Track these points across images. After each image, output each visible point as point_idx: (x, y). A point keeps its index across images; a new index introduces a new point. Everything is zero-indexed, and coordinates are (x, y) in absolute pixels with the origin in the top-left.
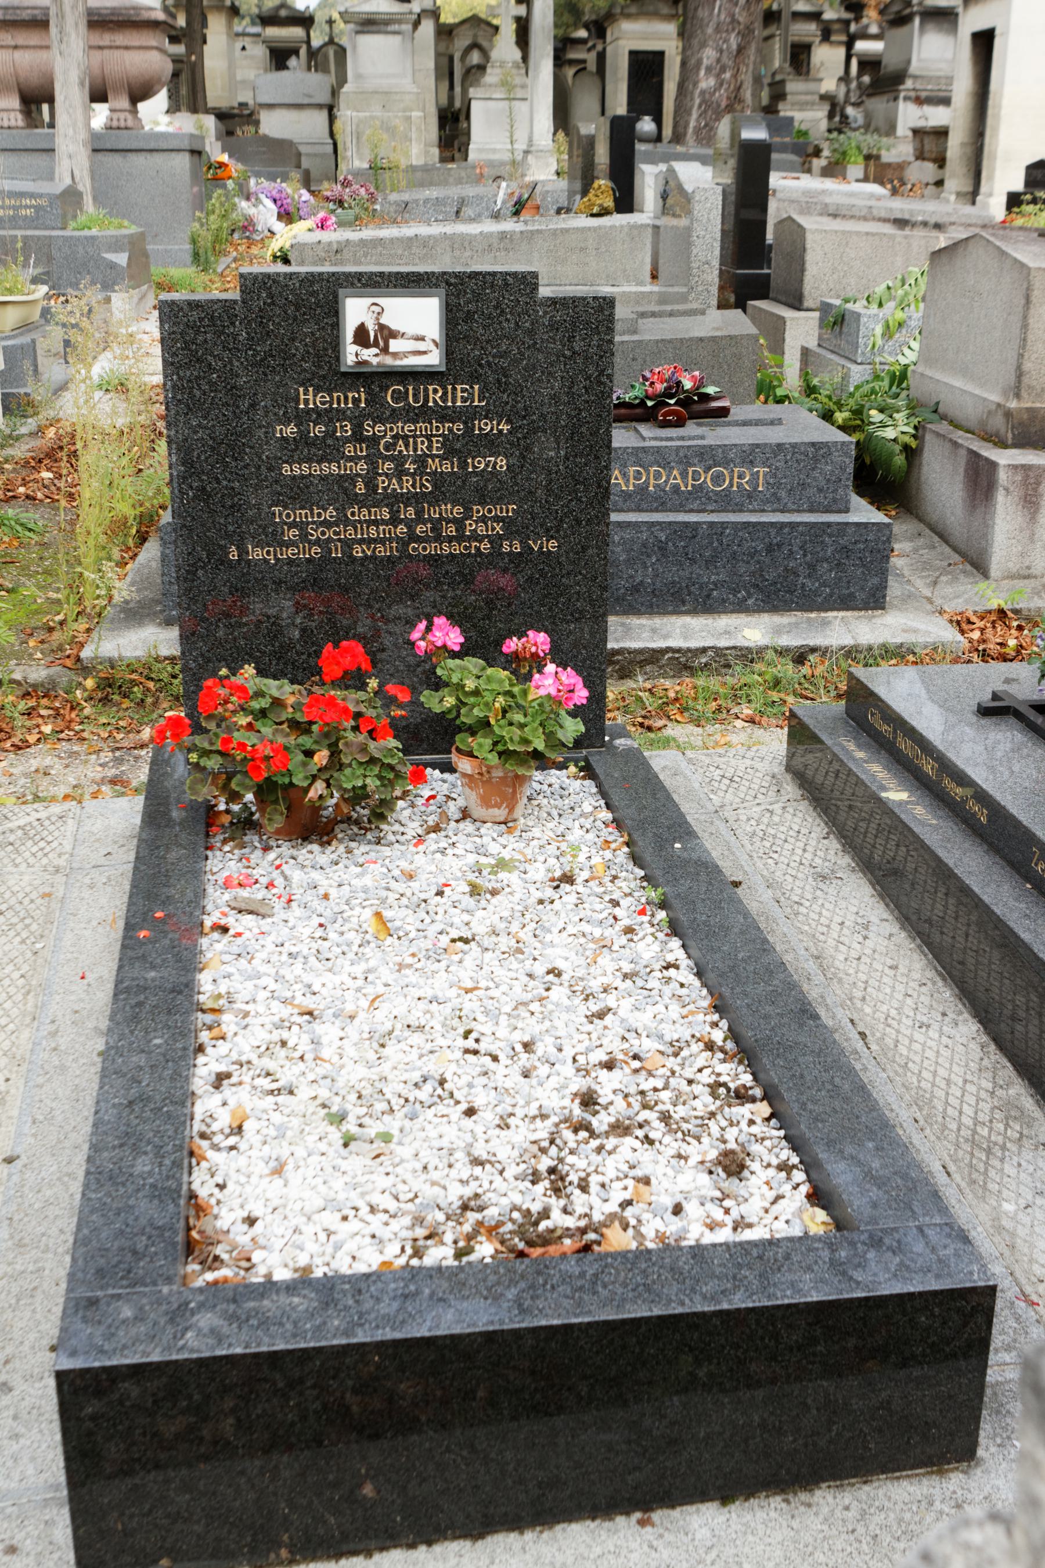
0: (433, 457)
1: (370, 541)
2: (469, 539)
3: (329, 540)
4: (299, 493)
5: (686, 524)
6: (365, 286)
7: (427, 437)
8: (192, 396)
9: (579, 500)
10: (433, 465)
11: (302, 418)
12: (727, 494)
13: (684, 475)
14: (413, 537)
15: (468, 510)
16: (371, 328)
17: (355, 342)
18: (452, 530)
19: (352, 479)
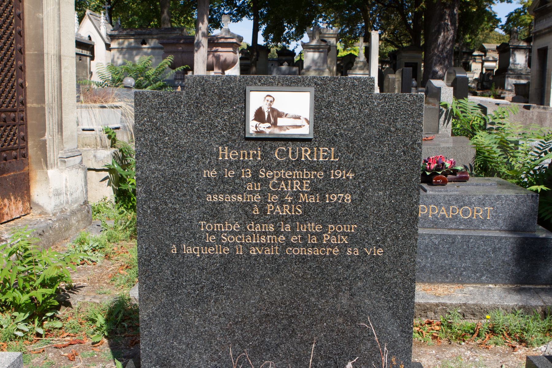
1: (261, 245)
2: (325, 246)
3: (235, 243)
4: (216, 213)
5: (450, 236)
6: (263, 84)
7: (299, 180)
8: (152, 151)
9: (398, 223)
10: (303, 198)
11: (219, 166)
12: (471, 220)
13: (448, 210)
14: (289, 244)
16: (266, 110)
17: (255, 119)
18: (314, 240)
19: (251, 205)
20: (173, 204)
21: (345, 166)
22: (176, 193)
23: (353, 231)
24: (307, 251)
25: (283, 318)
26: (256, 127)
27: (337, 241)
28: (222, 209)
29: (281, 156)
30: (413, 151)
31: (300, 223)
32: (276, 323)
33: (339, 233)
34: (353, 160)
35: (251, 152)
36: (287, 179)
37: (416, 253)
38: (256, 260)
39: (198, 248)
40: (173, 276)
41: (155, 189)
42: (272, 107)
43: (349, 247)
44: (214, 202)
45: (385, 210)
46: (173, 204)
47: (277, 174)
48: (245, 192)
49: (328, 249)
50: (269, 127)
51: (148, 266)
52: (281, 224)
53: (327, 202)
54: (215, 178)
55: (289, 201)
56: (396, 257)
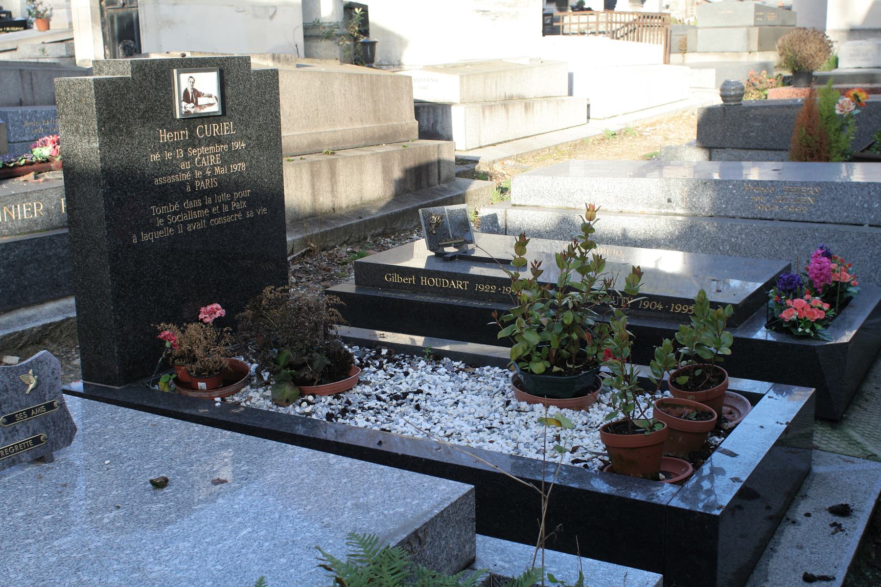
0: (216, 166)
6: (184, 67)
16: (190, 91)
18: (226, 209)
19: (183, 183)
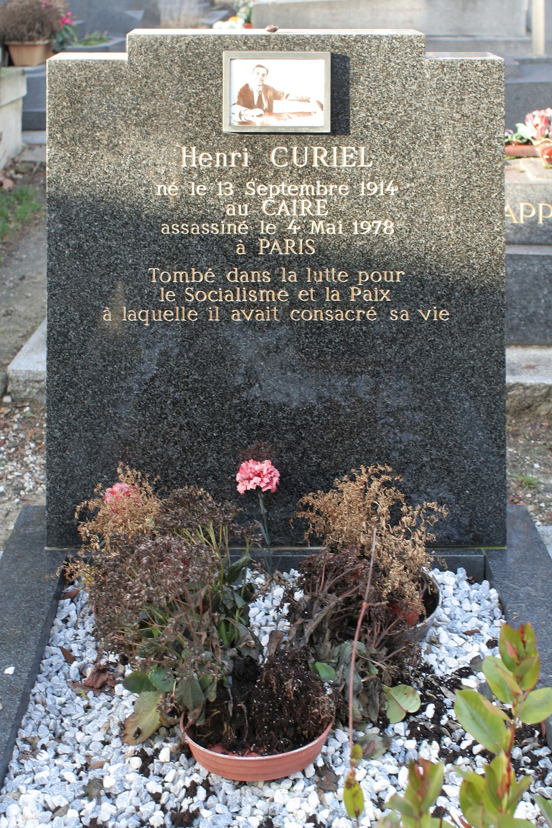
0: (317, 219)
1: (249, 306)
2: (355, 306)
6: (250, 48)
14: (294, 303)
15: (353, 275)
18: (336, 297)
19: (232, 240)
20: (107, 239)
21: (383, 175)
22: (112, 222)
23: (398, 280)
24: (324, 316)
25: (287, 431)
26: (240, 115)
27: (373, 298)
28: (186, 248)
29: (280, 161)
30: (490, 149)
31: (313, 269)
32: (275, 440)
33: (376, 285)
34: (394, 165)
35: (233, 155)
36: (290, 197)
37: (504, 317)
38: (241, 330)
39: (147, 312)
40: (105, 361)
41: (77, 215)
42: (265, 83)
43: (394, 308)
44: (174, 236)
45: (449, 245)
46: (107, 239)
47: (274, 190)
48: (223, 218)
49: (359, 312)
50: (260, 116)
51: (64, 342)
52: (281, 270)
53: (356, 233)
54: (174, 197)
55: (295, 232)
56: (470, 324)
